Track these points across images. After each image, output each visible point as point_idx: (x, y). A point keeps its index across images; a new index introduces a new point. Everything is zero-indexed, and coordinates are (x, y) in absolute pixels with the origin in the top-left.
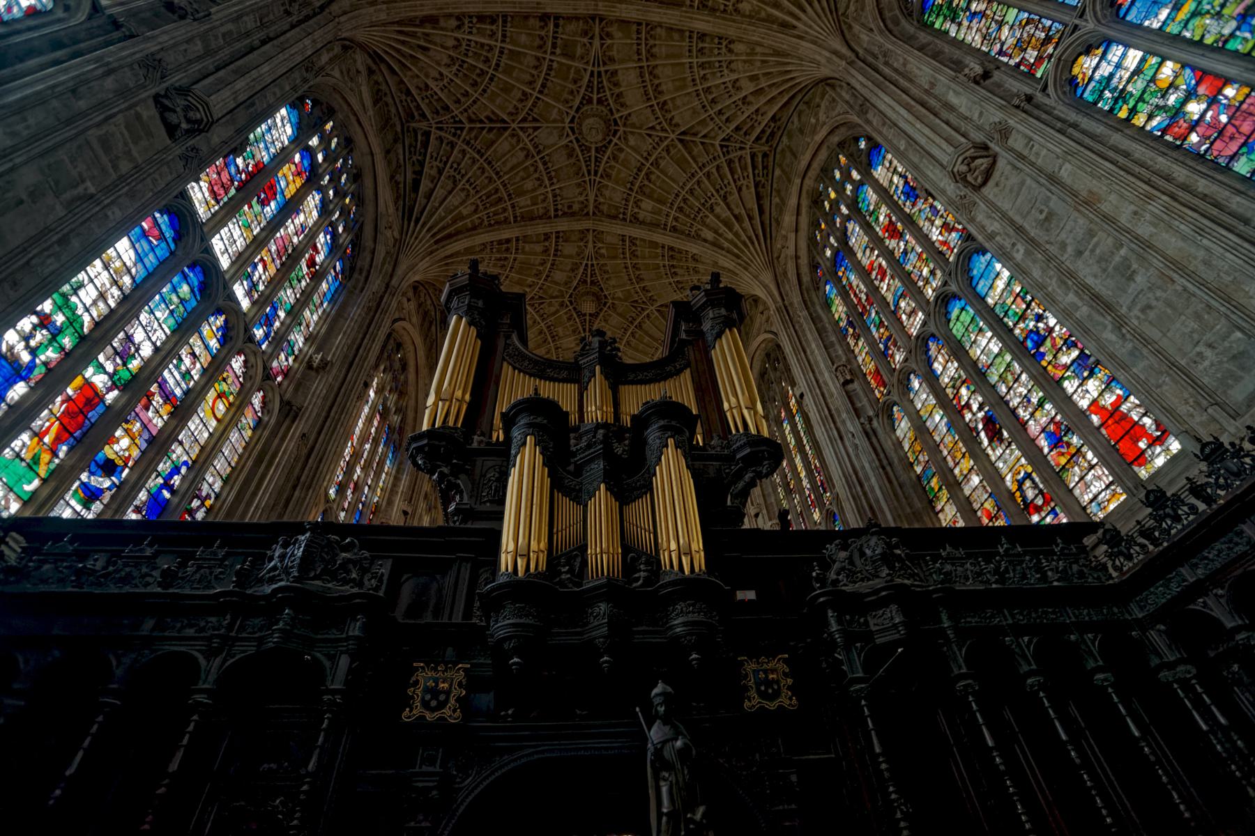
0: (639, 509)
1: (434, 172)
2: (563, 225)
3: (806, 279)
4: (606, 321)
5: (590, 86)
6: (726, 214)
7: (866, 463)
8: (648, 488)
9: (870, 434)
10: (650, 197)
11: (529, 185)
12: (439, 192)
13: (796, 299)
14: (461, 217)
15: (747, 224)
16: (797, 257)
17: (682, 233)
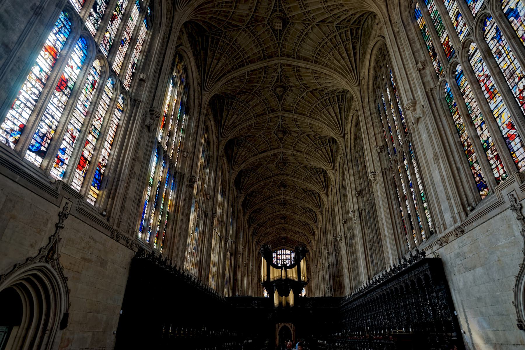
0: (288, 297)
1: (244, 178)
2: (275, 178)
3: (333, 207)
4: (287, 189)
5: (281, 158)
6: (316, 180)
7: (335, 262)
8: (289, 295)
9: (336, 256)
10: (297, 174)
11: (266, 174)
12: (245, 181)
13: (330, 213)
14: (250, 184)
15: (321, 184)
16: (331, 201)
17: (306, 181)
